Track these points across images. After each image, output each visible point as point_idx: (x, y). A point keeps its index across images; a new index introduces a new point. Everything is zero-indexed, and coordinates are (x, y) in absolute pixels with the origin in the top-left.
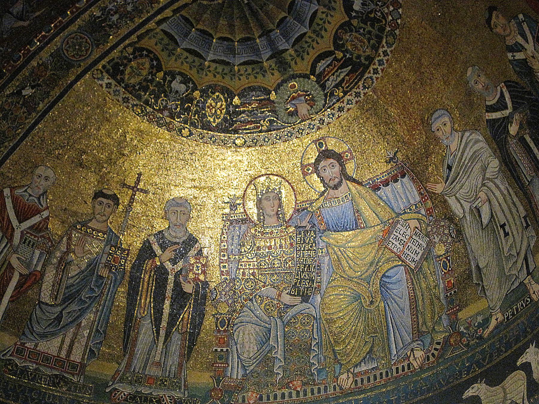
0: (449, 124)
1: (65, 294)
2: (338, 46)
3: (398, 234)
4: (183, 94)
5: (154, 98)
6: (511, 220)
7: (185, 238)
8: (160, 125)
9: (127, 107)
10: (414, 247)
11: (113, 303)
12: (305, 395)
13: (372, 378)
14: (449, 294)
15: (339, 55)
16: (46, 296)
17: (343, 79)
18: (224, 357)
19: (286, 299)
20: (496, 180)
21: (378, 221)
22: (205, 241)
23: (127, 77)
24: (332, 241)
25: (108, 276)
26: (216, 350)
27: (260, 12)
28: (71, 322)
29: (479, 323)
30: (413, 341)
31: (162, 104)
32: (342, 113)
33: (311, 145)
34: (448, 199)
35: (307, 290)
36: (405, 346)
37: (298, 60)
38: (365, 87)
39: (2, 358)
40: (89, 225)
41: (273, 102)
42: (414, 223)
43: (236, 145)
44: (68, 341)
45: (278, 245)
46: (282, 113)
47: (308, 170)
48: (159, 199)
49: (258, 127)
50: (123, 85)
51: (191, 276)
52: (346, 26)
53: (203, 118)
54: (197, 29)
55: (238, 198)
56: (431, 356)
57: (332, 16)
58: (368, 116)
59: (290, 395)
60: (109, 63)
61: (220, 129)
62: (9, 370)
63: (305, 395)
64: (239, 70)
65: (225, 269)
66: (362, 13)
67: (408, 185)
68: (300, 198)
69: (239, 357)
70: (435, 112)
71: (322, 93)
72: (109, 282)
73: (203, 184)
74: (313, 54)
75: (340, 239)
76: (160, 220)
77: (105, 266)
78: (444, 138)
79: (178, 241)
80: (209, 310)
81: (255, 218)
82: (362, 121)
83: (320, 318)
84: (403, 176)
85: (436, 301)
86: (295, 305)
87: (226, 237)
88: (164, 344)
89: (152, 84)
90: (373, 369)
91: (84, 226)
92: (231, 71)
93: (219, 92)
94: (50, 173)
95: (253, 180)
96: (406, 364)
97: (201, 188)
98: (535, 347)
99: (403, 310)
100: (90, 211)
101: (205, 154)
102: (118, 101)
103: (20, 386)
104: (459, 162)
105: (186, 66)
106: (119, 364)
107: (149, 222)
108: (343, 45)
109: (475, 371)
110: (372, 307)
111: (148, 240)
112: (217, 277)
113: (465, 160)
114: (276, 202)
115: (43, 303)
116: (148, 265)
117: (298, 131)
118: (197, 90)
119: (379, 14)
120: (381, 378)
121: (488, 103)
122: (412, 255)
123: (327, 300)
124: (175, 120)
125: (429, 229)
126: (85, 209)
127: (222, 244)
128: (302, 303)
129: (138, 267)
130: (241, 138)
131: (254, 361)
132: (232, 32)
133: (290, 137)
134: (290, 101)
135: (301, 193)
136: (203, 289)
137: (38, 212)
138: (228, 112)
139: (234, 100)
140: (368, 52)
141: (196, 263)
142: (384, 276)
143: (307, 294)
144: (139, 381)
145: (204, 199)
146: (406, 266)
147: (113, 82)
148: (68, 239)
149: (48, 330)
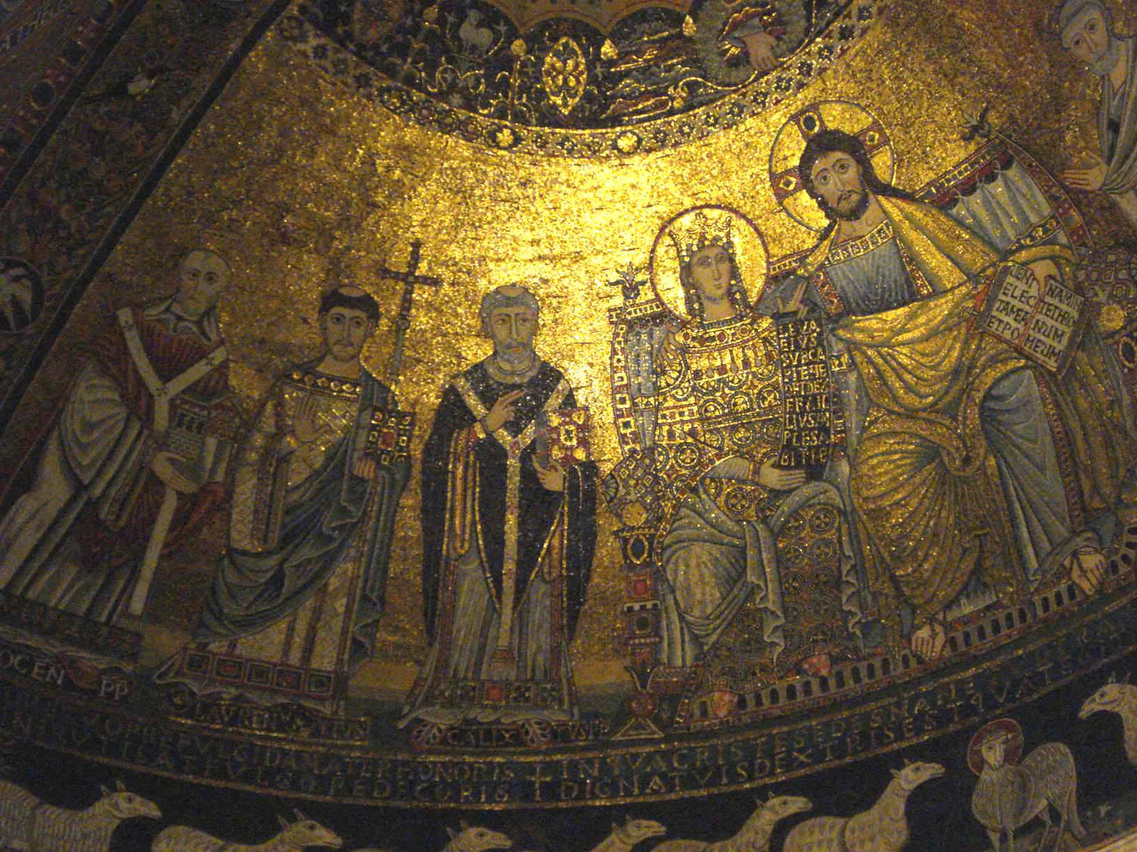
0: (1101, 26)
1: (284, 526)
3: (1009, 299)
4: (488, 51)
5: (424, 68)
8: (446, 129)
9: (369, 97)
10: (1050, 322)
11: (392, 532)
12: (841, 682)
13: (989, 630)
16: (242, 535)
18: (649, 622)
19: (772, 477)
21: (957, 276)
22: (576, 373)
23: (357, 27)
24: (859, 337)
25: (376, 477)
26: (630, 609)
28: (305, 587)
30: (1075, 533)
31: (445, 79)
32: (851, 42)
33: (788, 128)
34: (1118, 199)
35: (817, 453)
36: (1056, 546)
39: (158, 682)
40: (320, 369)
41: (690, 39)
42: (1043, 269)
43: (620, 151)
44: (301, 627)
45: (739, 362)
46: (714, 64)
47: (788, 184)
48: (466, 295)
49: (664, 104)
50: (352, 47)
51: (556, 453)
53: (539, 100)
55: (638, 270)
56: (1121, 563)
58: (910, 39)
61: (578, 120)
62: (177, 707)
63: (841, 682)
65: (629, 431)
67: (1020, 183)
68: (775, 250)
69: (682, 619)
72: (379, 489)
73: (557, 250)
75: (876, 330)
76: (473, 341)
77: (366, 455)
78: (1091, 58)
79: (517, 380)
80: (606, 523)
81: (681, 309)
82: (897, 53)
83: (854, 510)
84: (1007, 165)
85: (1117, 436)
86: (795, 489)
87: (622, 358)
88: (514, 608)
89: (415, 36)
90: (988, 608)
91: (307, 373)
93: (566, 34)
94: (216, 264)
95: (665, 226)
96: (1063, 586)
97: (553, 259)
99: (1041, 468)
100: (318, 340)
101: (555, 181)
102: (345, 84)
103: (205, 739)
107: (448, 347)
110: (969, 471)
111: (453, 389)
112: (614, 448)
114: (724, 267)
115: (236, 550)
116: (460, 441)
117: (755, 100)
118: (517, 38)
120: (1010, 626)
122: (1049, 341)
123: (864, 469)
124: (476, 112)
125: (1082, 275)
126: (305, 336)
127: (616, 376)
128: (807, 481)
129: (437, 449)
130: (629, 135)
131: (718, 622)
133: (739, 115)
134: (728, 33)
135: (778, 239)
136: (587, 478)
137: (202, 354)
138: (592, 80)
139: (603, 49)
141: (565, 423)
142: (988, 396)
143: (818, 460)
144: (468, 697)
145: (565, 282)
146: (1037, 367)
147: (331, 44)
148: (275, 406)
149: (253, 610)
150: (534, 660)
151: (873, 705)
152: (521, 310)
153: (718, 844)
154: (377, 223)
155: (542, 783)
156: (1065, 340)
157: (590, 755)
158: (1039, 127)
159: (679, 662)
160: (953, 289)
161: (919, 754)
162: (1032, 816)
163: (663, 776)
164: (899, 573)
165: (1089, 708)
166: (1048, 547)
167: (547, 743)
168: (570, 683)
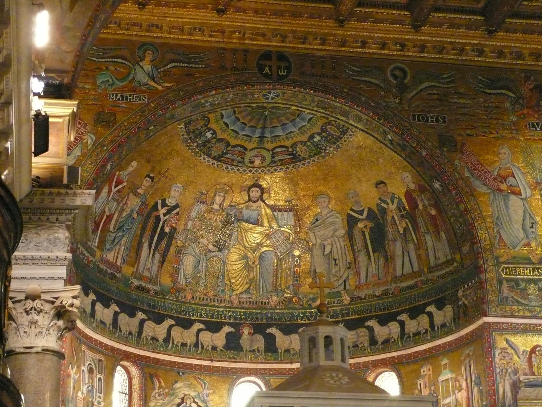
0: (326, 203)
2: (291, 147)
6: (341, 260)
12: (214, 301)
15: (290, 150)
19: (211, 247)
24: (242, 226)
30: (272, 292)
38: (293, 167)
44: (116, 252)
46: (247, 160)
52: (304, 143)
59: (207, 300)
61: (214, 158)
74: (279, 144)
84: (290, 211)
90: (249, 298)
104: (323, 221)
105: (219, 128)
106: (134, 267)
108: (296, 148)
114: (222, 198)
116: (154, 214)
121: (353, 208)
129: (149, 215)
138: (223, 152)
140: (306, 156)
151: (220, 309)
158: (302, 210)
163: (175, 310)
164: (232, 281)
165: (269, 331)
166: (265, 291)
168: (160, 281)
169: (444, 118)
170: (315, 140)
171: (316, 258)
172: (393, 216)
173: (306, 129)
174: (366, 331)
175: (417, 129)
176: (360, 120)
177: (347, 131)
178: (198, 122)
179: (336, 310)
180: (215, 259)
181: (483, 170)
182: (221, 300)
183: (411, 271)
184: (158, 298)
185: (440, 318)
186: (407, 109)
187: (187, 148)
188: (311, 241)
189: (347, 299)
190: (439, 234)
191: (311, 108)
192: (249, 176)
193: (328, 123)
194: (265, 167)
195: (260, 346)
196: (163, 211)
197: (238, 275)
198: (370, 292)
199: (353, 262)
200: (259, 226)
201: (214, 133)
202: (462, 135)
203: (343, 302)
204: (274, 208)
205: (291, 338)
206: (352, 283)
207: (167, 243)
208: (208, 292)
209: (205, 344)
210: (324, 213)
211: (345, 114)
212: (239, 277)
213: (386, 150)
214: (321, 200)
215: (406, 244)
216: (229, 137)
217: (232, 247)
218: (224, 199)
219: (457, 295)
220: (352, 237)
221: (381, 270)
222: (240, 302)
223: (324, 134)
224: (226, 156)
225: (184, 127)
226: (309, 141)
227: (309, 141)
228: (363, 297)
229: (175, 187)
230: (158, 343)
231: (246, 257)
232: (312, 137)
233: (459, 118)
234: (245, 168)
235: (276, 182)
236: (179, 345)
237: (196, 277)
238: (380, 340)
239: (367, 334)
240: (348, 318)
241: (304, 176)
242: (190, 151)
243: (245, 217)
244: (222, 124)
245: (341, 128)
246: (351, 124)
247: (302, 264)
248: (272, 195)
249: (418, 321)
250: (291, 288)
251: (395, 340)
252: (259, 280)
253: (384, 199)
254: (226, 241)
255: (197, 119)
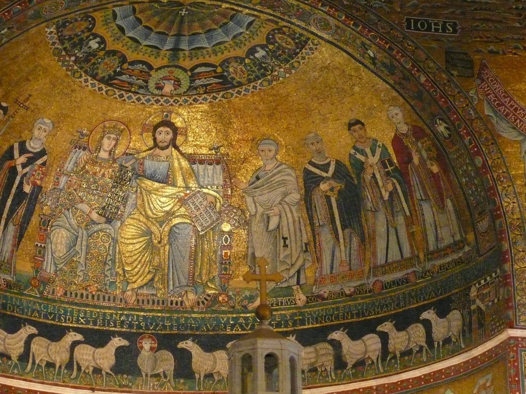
0: (273, 153)
2: (221, 65)
3: (195, 201)
6: (293, 239)
7: (38, 150)
10: (205, 216)
12: (98, 299)
14: (224, 262)
15: (219, 70)
17: (210, 84)
18: (41, 251)
19: (95, 216)
20: (292, 207)
24: (143, 185)
26: (37, 245)
27: (186, 23)
29: (246, 296)
30: (188, 286)
34: (246, 196)
37: (188, 59)
38: (223, 96)
41: (151, 76)
46: (152, 85)
52: (240, 60)
54: (135, 17)
56: (201, 303)
57: (234, 49)
59: (87, 297)
60: (62, 20)
61: (101, 80)
64: (142, 49)
66: (259, 61)
69: (52, 255)
70: (267, 139)
71: (189, 84)
74: (201, 60)
84: (218, 163)
86: (100, 223)
90: (153, 295)
92: (136, 47)
98: (296, 339)
105: (110, 34)
108: (228, 67)
109: (238, 330)
113: (274, 180)
114: (114, 143)
116: (7, 164)
119: (270, 67)
120: (158, 304)
121: (313, 160)
122: (202, 221)
128: (106, 223)
132: (156, 27)
138: (115, 72)
140: (243, 81)
142: (174, 226)
150: (5, 255)
151: (107, 311)
152: (47, 128)
153: (54, 343)
154: (24, 86)
155: (3, 303)
156: (208, 224)
157: (16, 296)
158: (235, 162)
159: (48, 271)
160: (179, 187)
161: (121, 334)
162: (157, 372)
163: (38, 312)
164: (126, 269)
165: (181, 345)
166: (177, 284)
167: (5, 287)
168: (15, 268)
169: (454, 26)
170: (257, 55)
171: (255, 236)
172: (374, 174)
173: (243, 39)
174: (330, 348)
175: (413, 42)
176: (326, 26)
177: (306, 42)
178: (77, 24)
179: (285, 315)
180: (101, 234)
181: (512, 106)
182: (109, 297)
183: (399, 258)
184: (11, 293)
185: (442, 330)
186: (399, 10)
187: (60, 63)
188: (248, 210)
189: (301, 298)
190: (442, 200)
191: (252, 6)
192: (155, 109)
193: (278, 29)
194: (180, 95)
195: (167, 367)
196: (20, 160)
197: (135, 260)
198: (337, 288)
199: (312, 244)
200: (169, 185)
201: (103, 41)
202: (481, 51)
203: (295, 304)
204: (192, 159)
205: (215, 357)
206: (309, 275)
207: (27, 210)
208: (89, 285)
209: (84, 365)
210: (269, 167)
211: (302, 16)
212: (137, 262)
213: (365, 74)
214: (265, 147)
215: (393, 217)
216: (125, 47)
217: (128, 217)
218: (117, 142)
219: (468, 295)
220: (311, 204)
221: (354, 254)
222: (138, 300)
223: (271, 47)
224: (119, 78)
225: (55, 31)
226: (247, 56)
227: (247, 56)
228: (326, 295)
229: (40, 123)
230: (10, 363)
231: (149, 233)
232: (252, 51)
233: (477, 26)
234: (150, 97)
235: (196, 119)
236: (43, 365)
237: (70, 262)
238: (350, 361)
239: (332, 352)
240: (302, 327)
241: (240, 111)
242: (64, 68)
243: (148, 172)
244: (115, 27)
245: (298, 38)
246: (313, 33)
247: (234, 244)
248: (190, 139)
249: (408, 334)
250: (217, 280)
251: (373, 362)
252: (169, 267)
253: (359, 146)
254: (118, 208)
255: (76, 20)
